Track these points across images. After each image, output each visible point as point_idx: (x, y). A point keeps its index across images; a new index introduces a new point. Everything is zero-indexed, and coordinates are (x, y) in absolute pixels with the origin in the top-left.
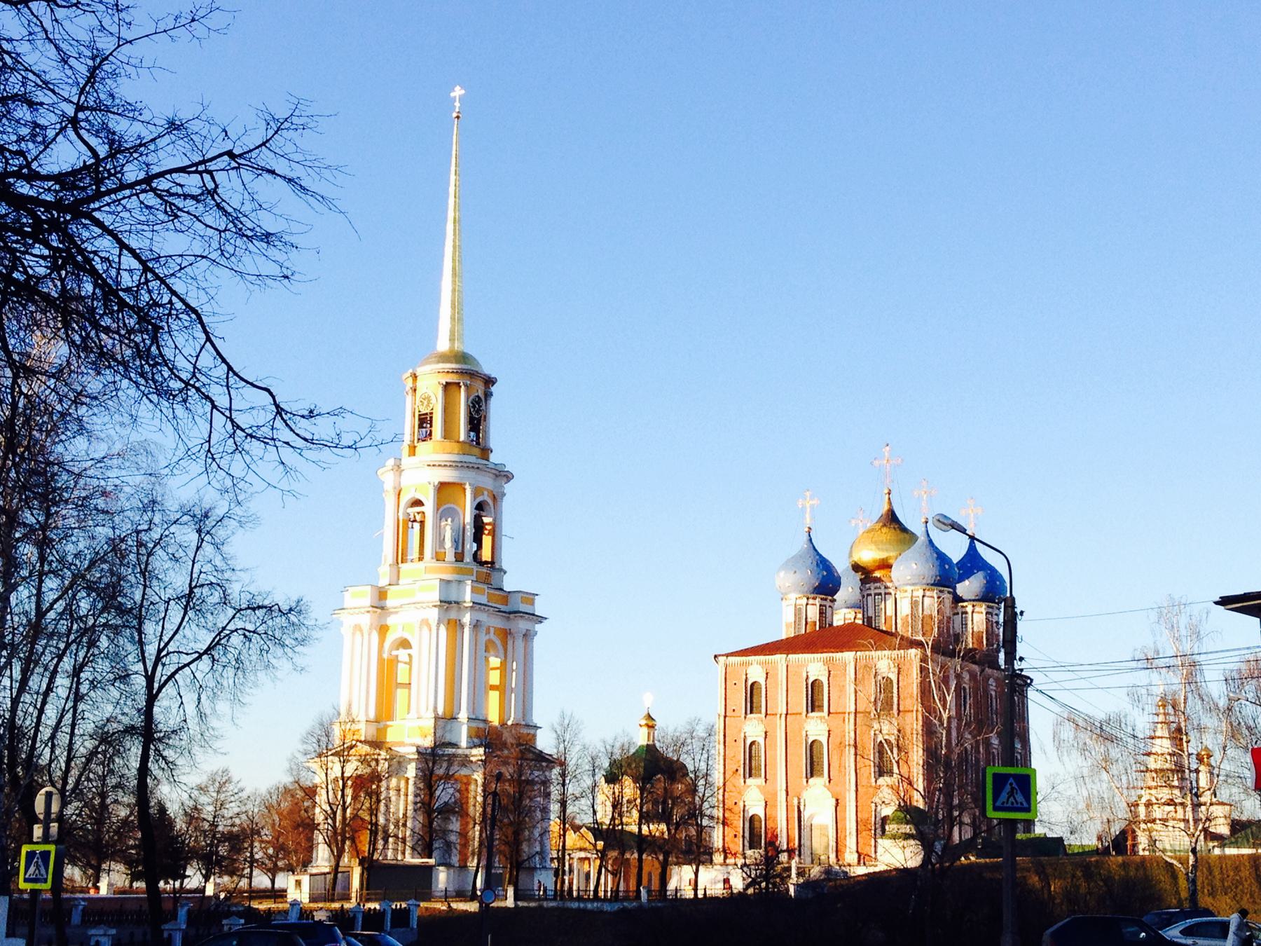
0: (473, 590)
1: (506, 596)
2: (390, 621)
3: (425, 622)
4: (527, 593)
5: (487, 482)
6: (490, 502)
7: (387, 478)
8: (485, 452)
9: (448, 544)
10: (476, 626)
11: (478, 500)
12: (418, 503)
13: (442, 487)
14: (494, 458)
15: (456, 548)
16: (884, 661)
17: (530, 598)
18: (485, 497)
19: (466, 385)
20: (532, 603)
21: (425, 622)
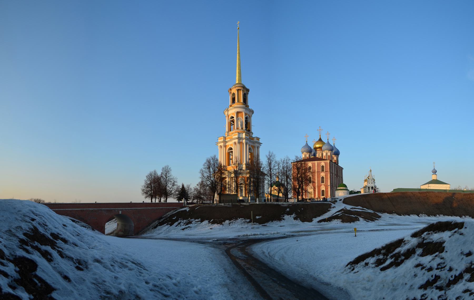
0: (246, 135)
1: (253, 138)
2: (227, 144)
3: (235, 143)
4: (258, 138)
5: (248, 112)
6: (249, 117)
7: (226, 113)
8: (247, 106)
9: (239, 126)
10: (246, 144)
11: (246, 116)
12: (233, 117)
13: (238, 113)
14: (250, 108)
15: (241, 127)
16: (323, 163)
17: (258, 139)
18: (247, 116)
19: (243, 90)
20: (259, 140)
21: (235, 143)
